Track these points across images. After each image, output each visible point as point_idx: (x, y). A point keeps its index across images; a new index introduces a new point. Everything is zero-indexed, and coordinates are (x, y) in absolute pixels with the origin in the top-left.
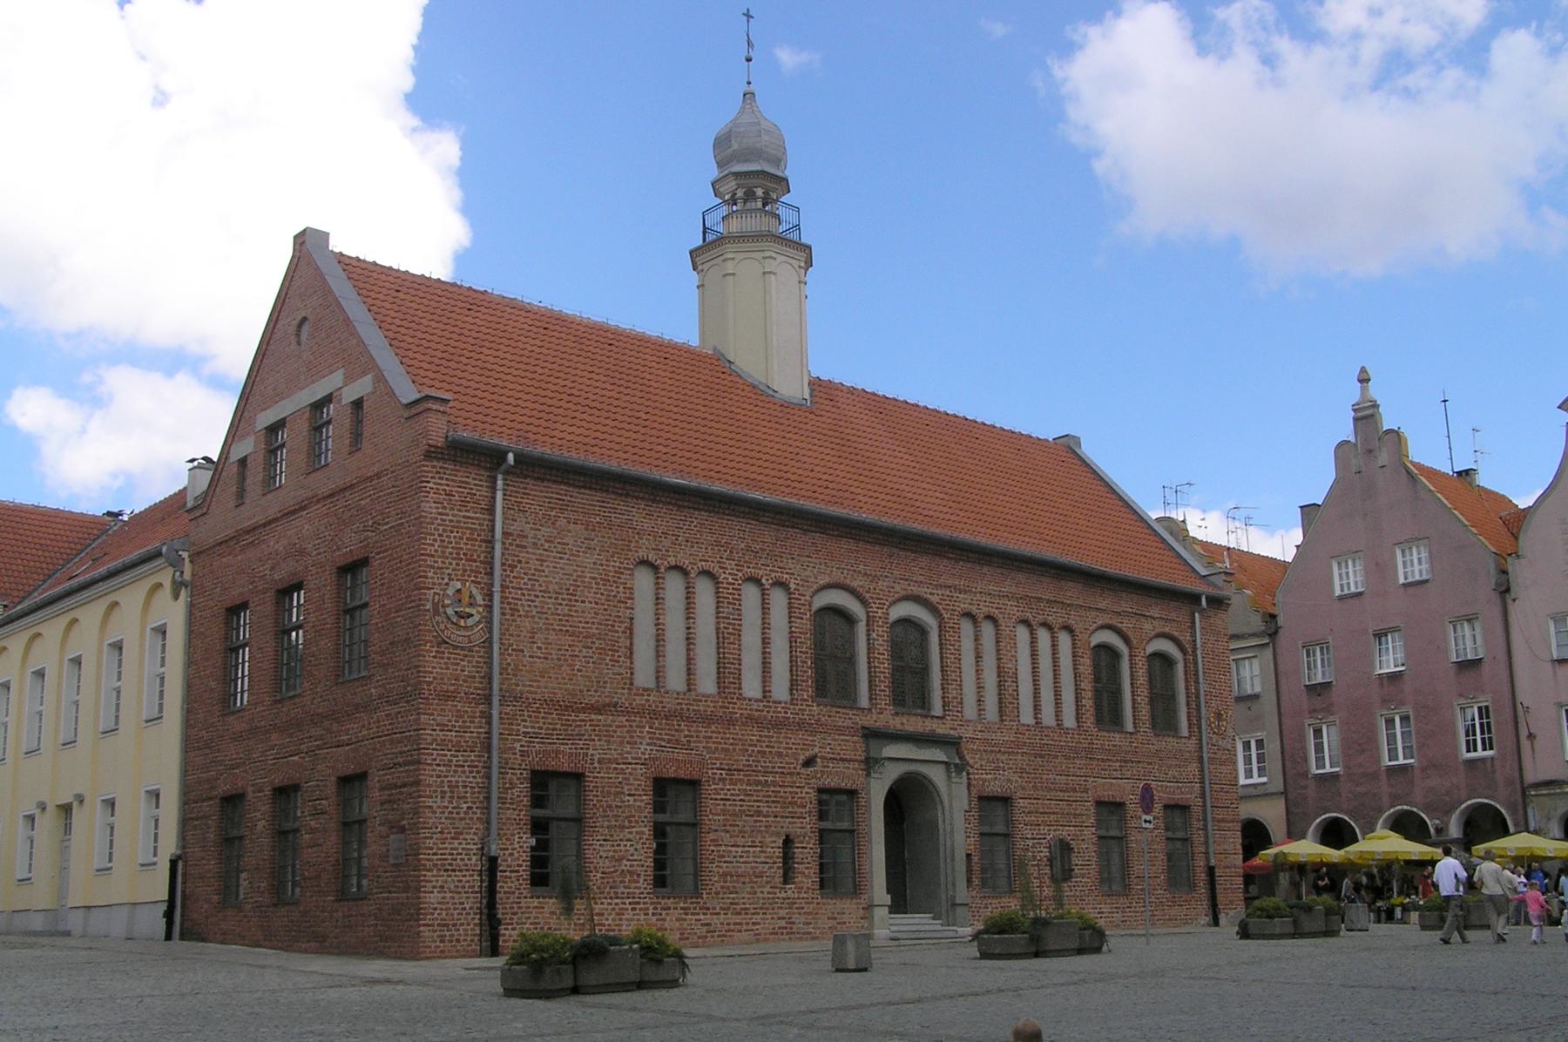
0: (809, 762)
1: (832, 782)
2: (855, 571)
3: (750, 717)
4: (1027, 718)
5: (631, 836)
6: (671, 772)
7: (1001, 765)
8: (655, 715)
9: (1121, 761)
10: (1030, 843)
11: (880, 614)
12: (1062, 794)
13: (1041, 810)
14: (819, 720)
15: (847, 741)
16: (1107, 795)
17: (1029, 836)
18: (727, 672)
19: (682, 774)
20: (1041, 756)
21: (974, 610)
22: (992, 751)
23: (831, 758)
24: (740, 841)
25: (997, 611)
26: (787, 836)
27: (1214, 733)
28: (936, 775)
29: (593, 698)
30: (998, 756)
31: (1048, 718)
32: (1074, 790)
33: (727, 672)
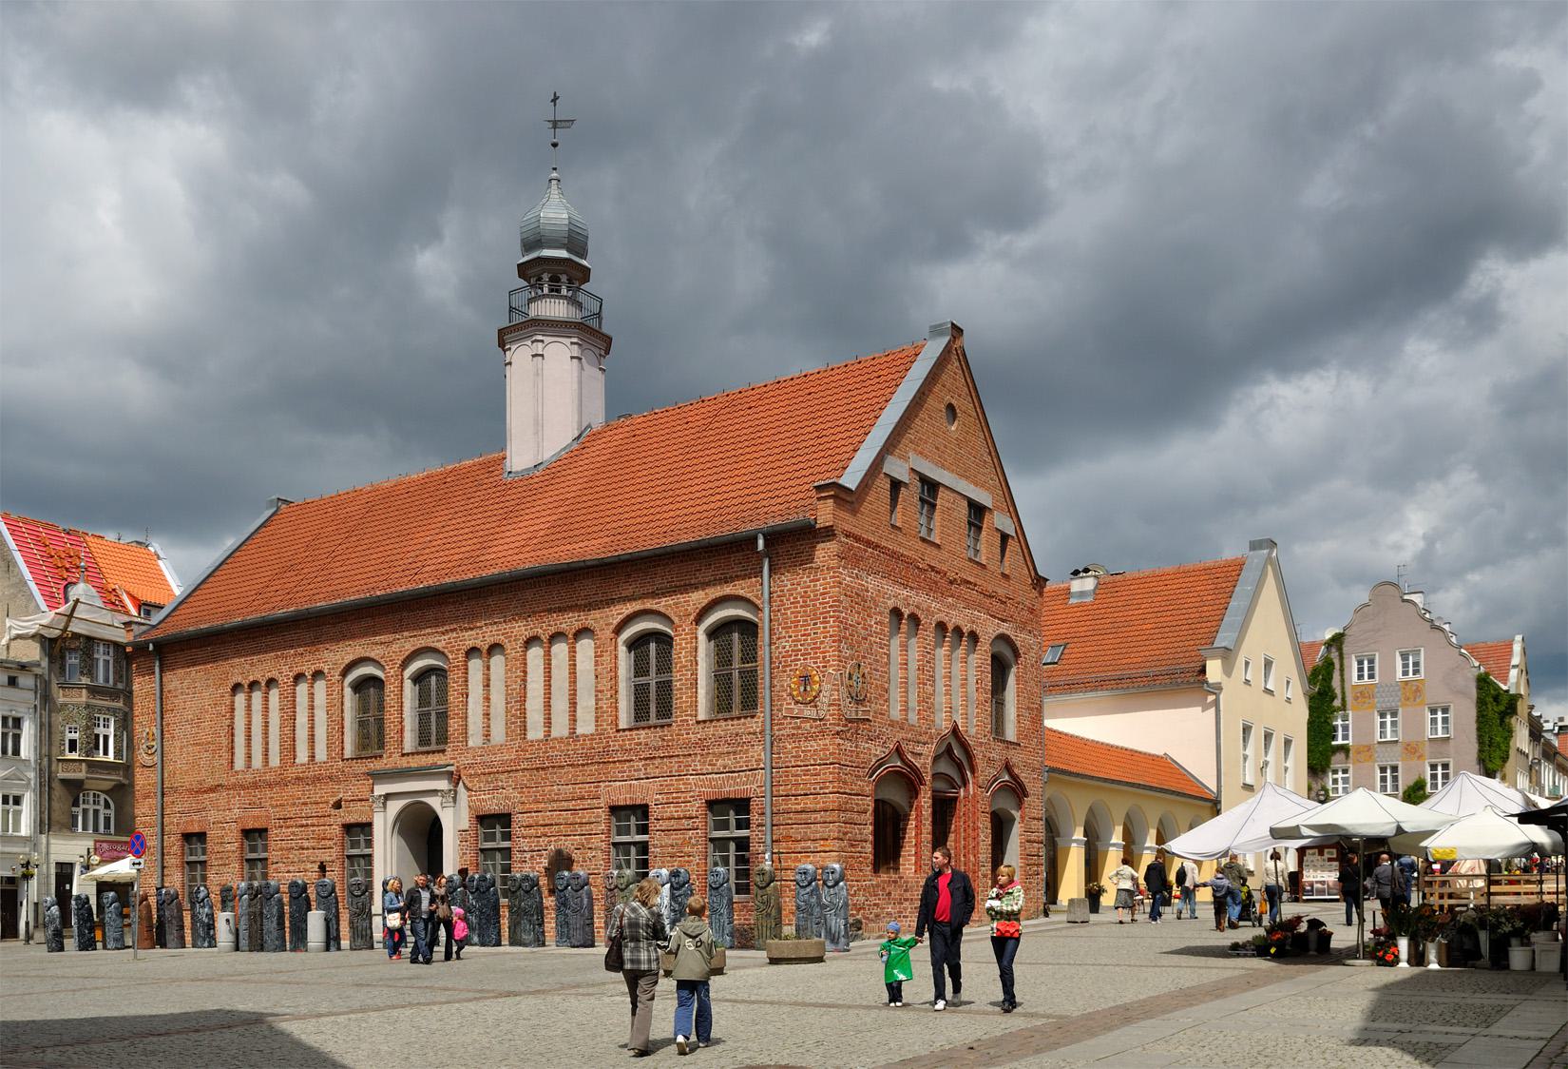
0: (338, 805)
1: (352, 819)
2: (373, 643)
3: (298, 778)
4: (536, 733)
5: (229, 870)
6: (250, 826)
7: (500, 784)
8: (243, 787)
9: (646, 759)
10: (528, 855)
11: (392, 673)
12: (566, 804)
13: (541, 822)
14: (343, 771)
15: (364, 784)
16: (623, 799)
17: (527, 849)
18: (289, 749)
19: (257, 826)
20: (543, 769)
21: (478, 643)
22: (490, 774)
23: (352, 800)
24: (291, 868)
25: (502, 638)
26: (322, 863)
27: (797, 702)
28: (434, 802)
29: (211, 782)
30: (497, 775)
31: (561, 728)
32: (582, 798)
33: (289, 749)
